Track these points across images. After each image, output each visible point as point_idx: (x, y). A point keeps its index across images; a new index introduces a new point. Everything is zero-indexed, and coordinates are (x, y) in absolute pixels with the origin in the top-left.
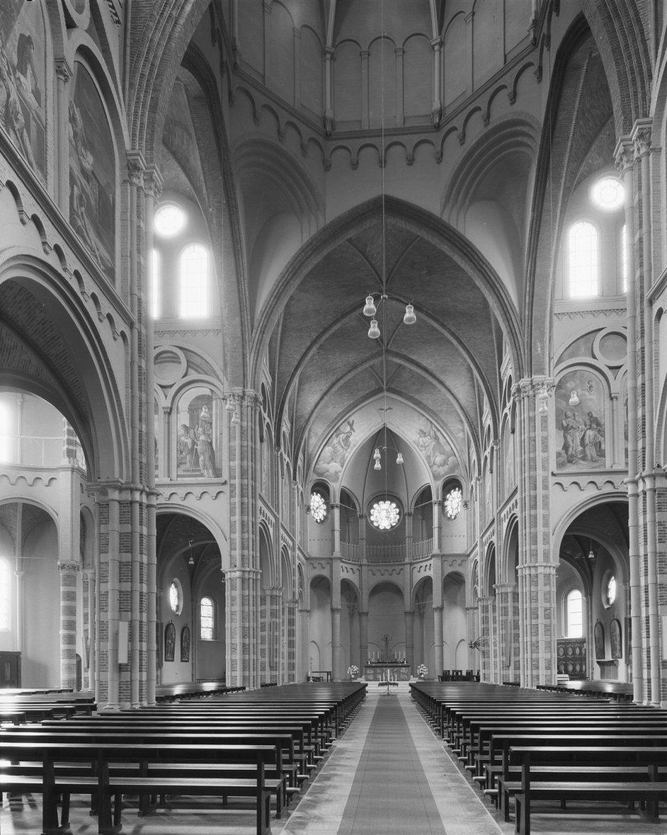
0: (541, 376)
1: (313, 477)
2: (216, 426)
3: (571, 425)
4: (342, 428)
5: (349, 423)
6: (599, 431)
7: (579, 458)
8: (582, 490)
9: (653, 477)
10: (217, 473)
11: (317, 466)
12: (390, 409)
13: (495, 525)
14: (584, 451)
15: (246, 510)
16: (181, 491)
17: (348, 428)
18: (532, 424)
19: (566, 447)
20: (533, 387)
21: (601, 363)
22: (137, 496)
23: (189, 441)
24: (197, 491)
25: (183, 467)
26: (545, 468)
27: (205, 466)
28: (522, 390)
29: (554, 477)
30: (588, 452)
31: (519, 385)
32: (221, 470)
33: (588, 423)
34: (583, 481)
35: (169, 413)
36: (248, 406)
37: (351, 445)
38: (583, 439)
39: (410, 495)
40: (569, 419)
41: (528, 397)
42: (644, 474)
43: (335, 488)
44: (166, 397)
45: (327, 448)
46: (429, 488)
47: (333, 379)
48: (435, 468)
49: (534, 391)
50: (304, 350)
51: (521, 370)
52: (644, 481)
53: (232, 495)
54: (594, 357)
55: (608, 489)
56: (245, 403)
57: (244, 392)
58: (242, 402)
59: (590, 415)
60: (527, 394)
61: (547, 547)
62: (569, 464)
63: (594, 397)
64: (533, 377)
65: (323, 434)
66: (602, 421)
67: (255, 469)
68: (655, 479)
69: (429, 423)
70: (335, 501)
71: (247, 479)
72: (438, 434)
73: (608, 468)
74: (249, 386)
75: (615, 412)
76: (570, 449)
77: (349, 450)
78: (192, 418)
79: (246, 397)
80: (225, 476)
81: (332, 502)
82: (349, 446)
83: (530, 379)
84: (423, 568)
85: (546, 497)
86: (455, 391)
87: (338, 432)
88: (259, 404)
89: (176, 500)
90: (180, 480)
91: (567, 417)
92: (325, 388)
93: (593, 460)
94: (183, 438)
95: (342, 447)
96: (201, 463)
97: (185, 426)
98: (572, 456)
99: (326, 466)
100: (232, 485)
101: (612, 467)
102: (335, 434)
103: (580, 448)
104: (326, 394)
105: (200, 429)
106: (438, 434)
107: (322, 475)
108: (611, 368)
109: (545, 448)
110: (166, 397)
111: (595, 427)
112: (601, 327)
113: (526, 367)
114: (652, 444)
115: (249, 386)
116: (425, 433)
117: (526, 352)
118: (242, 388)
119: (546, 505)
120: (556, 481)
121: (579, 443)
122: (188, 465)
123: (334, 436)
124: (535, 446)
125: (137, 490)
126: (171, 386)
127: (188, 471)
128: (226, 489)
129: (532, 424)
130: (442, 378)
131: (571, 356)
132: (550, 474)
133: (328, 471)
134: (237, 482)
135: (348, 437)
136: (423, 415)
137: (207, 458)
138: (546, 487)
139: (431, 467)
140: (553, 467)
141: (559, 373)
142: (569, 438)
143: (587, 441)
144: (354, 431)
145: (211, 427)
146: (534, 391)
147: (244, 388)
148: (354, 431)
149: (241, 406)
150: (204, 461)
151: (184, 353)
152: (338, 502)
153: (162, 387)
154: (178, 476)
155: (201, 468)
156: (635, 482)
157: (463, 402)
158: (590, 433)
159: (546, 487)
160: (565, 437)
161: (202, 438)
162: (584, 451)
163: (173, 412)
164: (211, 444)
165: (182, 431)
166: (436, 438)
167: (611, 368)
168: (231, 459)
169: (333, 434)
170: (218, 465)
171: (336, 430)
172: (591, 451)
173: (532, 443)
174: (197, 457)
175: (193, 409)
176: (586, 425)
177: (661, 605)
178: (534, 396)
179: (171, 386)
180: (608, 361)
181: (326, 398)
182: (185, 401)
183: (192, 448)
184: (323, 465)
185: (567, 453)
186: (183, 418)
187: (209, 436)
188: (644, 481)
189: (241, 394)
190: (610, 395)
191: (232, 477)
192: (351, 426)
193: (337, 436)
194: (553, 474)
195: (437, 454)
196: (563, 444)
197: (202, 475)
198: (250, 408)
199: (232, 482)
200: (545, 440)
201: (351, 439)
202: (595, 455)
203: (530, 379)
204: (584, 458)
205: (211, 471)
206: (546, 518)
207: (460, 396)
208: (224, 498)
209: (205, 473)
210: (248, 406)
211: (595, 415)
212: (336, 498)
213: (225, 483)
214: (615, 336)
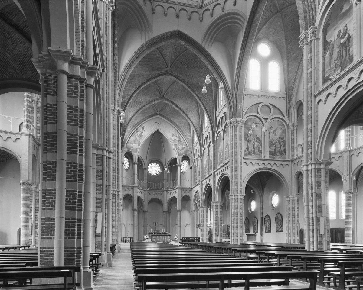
0: (240, 118)
1: (126, 150)
3: (249, 139)
4: (139, 129)
5: (142, 127)
6: (260, 143)
7: (252, 153)
8: (278, 167)
9: (315, 164)
11: (127, 145)
12: (160, 123)
13: (212, 176)
14: (254, 150)
15: (115, 163)
17: (142, 129)
18: (236, 137)
19: (248, 148)
20: (237, 122)
21: (261, 116)
22: (105, 153)
26: (241, 156)
29: (244, 160)
30: (256, 151)
33: (256, 140)
34: (254, 162)
36: (116, 115)
37: (143, 137)
38: (254, 145)
39: (166, 161)
41: (235, 126)
42: (312, 162)
43: (136, 155)
45: (132, 137)
46: (176, 159)
47: (140, 107)
48: (179, 151)
50: (133, 92)
51: (232, 115)
52: (311, 165)
54: (258, 113)
55: (263, 166)
56: (115, 113)
57: (114, 108)
58: (113, 112)
59: (256, 136)
60: (234, 125)
61: (241, 187)
62: (249, 155)
64: (237, 118)
65: (130, 131)
68: (316, 165)
69: (177, 132)
70: (135, 161)
71: (116, 148)
72: (180, 136)
73: (263, 158)
74: (117, 105)
75: (265, 136)
77: (142, 139)
81: (134, 161)
82: (142, 137)
83: (235, 119)
84: (172, 193)
85: (241, 168)
86: (192, 119)
87: (137, 130)
92: (136, 110)
93: (257, 154)
95: (139, 137)
98: (250, 152)
99: (131, 145)
101: (264, 157)
102: (136, 131)
103: (253, 149)
104: (136, 113)
106: (180, 136)
107: (130, 149)
108: (264, 119)
109: (241, 148)
112: (261, 102)
113: (233, 113)
114: (315, 151)
115: (117, 105)
116: (175, 135)
117: (234, 107)
118: (114, 106)
119: (241, 171)
120: (256, 162)
123: (135, 132)
124: (237, 146)
125: (105, 150)
129: (236, 137)
130: (186, 112)
131: (250, 112)
133: (132, 148)
135: (141, 133)
136: (174, 128)
138: (241, 163)
139: (177, 150)
140: (243, 156)
141: (248, 116)
143: (255, 147)
144: (144, 131)
148: (144, 131)
149: (113, 114)
152: (137, 162)
156: (307, 166)
157: (195, 124)
158: (256, 143)
159: (241, 163)
160: (247, 144)
162: (254, 150)
166: (179, 138)
167: (264, 119)
169: (135, 131)
171: (136, 129)
172: (257, 151)
173: (236, 145)
176: (255, 140)
177: (318, 213)
178: (237, 126)
181: (136, 115)
184: (130, 145)
185: (248, 150)
188: (311, 165)
192: (143, 128)
193: (137, 132)
194: (243, 158)
195: (180, 145)
198: (117, 116)
201: (143, 134)
202: (258, 152)
204: (254, 153)
206: (241, 176)
207: (194, 122)
212: (136, 160)
214: (267, 107)
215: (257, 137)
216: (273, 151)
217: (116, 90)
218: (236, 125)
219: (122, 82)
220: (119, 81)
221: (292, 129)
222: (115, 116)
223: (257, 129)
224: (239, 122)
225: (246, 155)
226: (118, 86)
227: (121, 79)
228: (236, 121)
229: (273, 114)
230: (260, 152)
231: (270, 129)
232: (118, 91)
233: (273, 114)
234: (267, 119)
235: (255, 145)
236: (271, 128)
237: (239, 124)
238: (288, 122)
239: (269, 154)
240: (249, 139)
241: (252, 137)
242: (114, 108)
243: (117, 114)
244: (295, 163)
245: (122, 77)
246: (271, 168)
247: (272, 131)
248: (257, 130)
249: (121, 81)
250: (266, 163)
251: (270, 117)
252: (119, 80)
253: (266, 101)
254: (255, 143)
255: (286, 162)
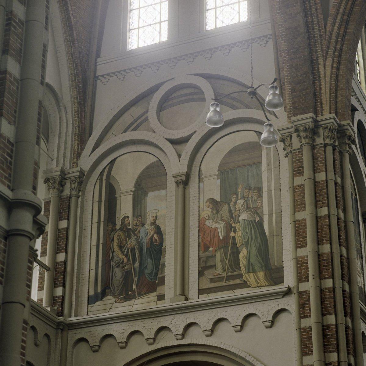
2: (269, 191)
10: (275, 276)
16: (205, 319)
23: (220, 227)
24: (235, 314)
25: (210, 274)
27: (250, 268)
32: (280, 269)
35: (184, 182)
44: (179, 156)
53: (303, 313)
56: (320, 141)
58: (314, 140)
67: (348, 259)
78: (224, 189)
79: (321, 130)
80: (289, 278)
88: (348, 142)
89: (196, 337)
90: (205, 299)
94: (209, 223)
96: (243, 262)
97: (212, 201)
100: (303, 296)
105: (241, 202)
110: (179, 156)
118: (311, 115)
122: (219, 270)
126: (186, 140)
127: (221, 279)
128: (291, 303)
134: (310, 286)
137: (254, 251)
145: (260, 196)
147: (316, 114)
150: (249, 257)
151: (210, 83)
153: (173, 142)
154: (201, 292)
155: (243, 270)
161: (244, 216)
163: (191, 183)
164: (260, 224)
165: (207, 211)
168: (300, 243)
170: (275, 262)
174: (236, 253)
175: (225, 171)
179: (186, 140)
182: (211, 163)
183: (227, 237)
186: (212, 189)
187: (257, 211)
189: (312, 125)
191: (302, 277)
197: (245, 285)
198: (329, 149)
199: (303, 287)
205: (261, 274)
208: (289, 324)
209: (250, 278)
210: (325, 146)
213: (289, 292)
217: (321, 61)
219: (343, 27)
220: (329, 27)
222: (320, 154)
226: (325, 43)
227: (339, 16)
232: (329, 61)
242: (315, 121)
243: (328, 141)
245: (341, 10)
249: (337, 25)
252: (330, 21)
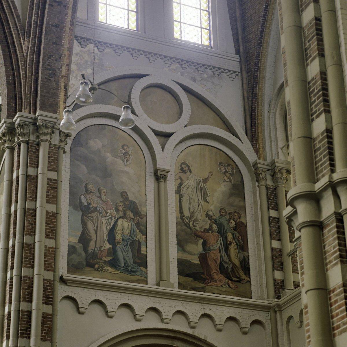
3: (93, 205)
6: (138, 225)
7: (105, 262)
14: (113, 252)
19: (84, 239)
20: (37, 128)
26: (50, 264)
28: (18, 131)
30: (120, 254)
31: (13, 123)
33: (120, 208)
34: (112, 300)
40: (93, 197)
41: (27, 143)
49: (38, 137)
55: (151, 322)
59: (124, 195)
62: (89, 269)
63: (130, 170)
66: (142, 210)
73: (151, 285)
76: (92, 244)
83: (32, 115)
91: (88, 191)
93: (128, 270)
98: (94, 255)
103: (108, 246)
108: (158, 134)
109: (52, 231)
111: (132, 216)
112: (147, 74)
121: (105, 237)
124: (34, 224)
132: (57, 279)
138: (49, 298)
140: (62, 268)
142: (90, 226)
143: (119, 237)
146: (38, 137)
158: (124, 225)
160: (84, 223)
162: (113, 252)
167: (158, 134)
172: (124, 254)
173: (31, 219)
176: (117, 210)
178: (38, 144)
180: (152, 121)
190: (156, 171)
194: (62, 280)
196: (79, 233)
200: (52, 220)
202: (130, 261)
203: (32, 115)
204: (114, 263)
211: (131, 197)
214: (169, 96)
215: (127, 199)
216: (195, 260)
218: (32, 138)
221: (270, 182)
223: (127, 169)
224: (46, 127)
225: (73, 268)
228: (35, 124)
229: (191, 123)
230: (143, 262)
231: (184, 176)
233: (191, 123)
234: (168, 136)
235: (118, 230)
236: (183, 171)
237: (45, 134)
238: (252, 157)
239: (181, 273)
240: (93, 205)
241: (104, 198)
244: (291, 317)
246: (190, 331)
247: (190, 182)
248: (127, 173)
250: (168, 308)
251: (180, 129)
253: (166, 76)
254: (120, 222)
255: (256, 312)
